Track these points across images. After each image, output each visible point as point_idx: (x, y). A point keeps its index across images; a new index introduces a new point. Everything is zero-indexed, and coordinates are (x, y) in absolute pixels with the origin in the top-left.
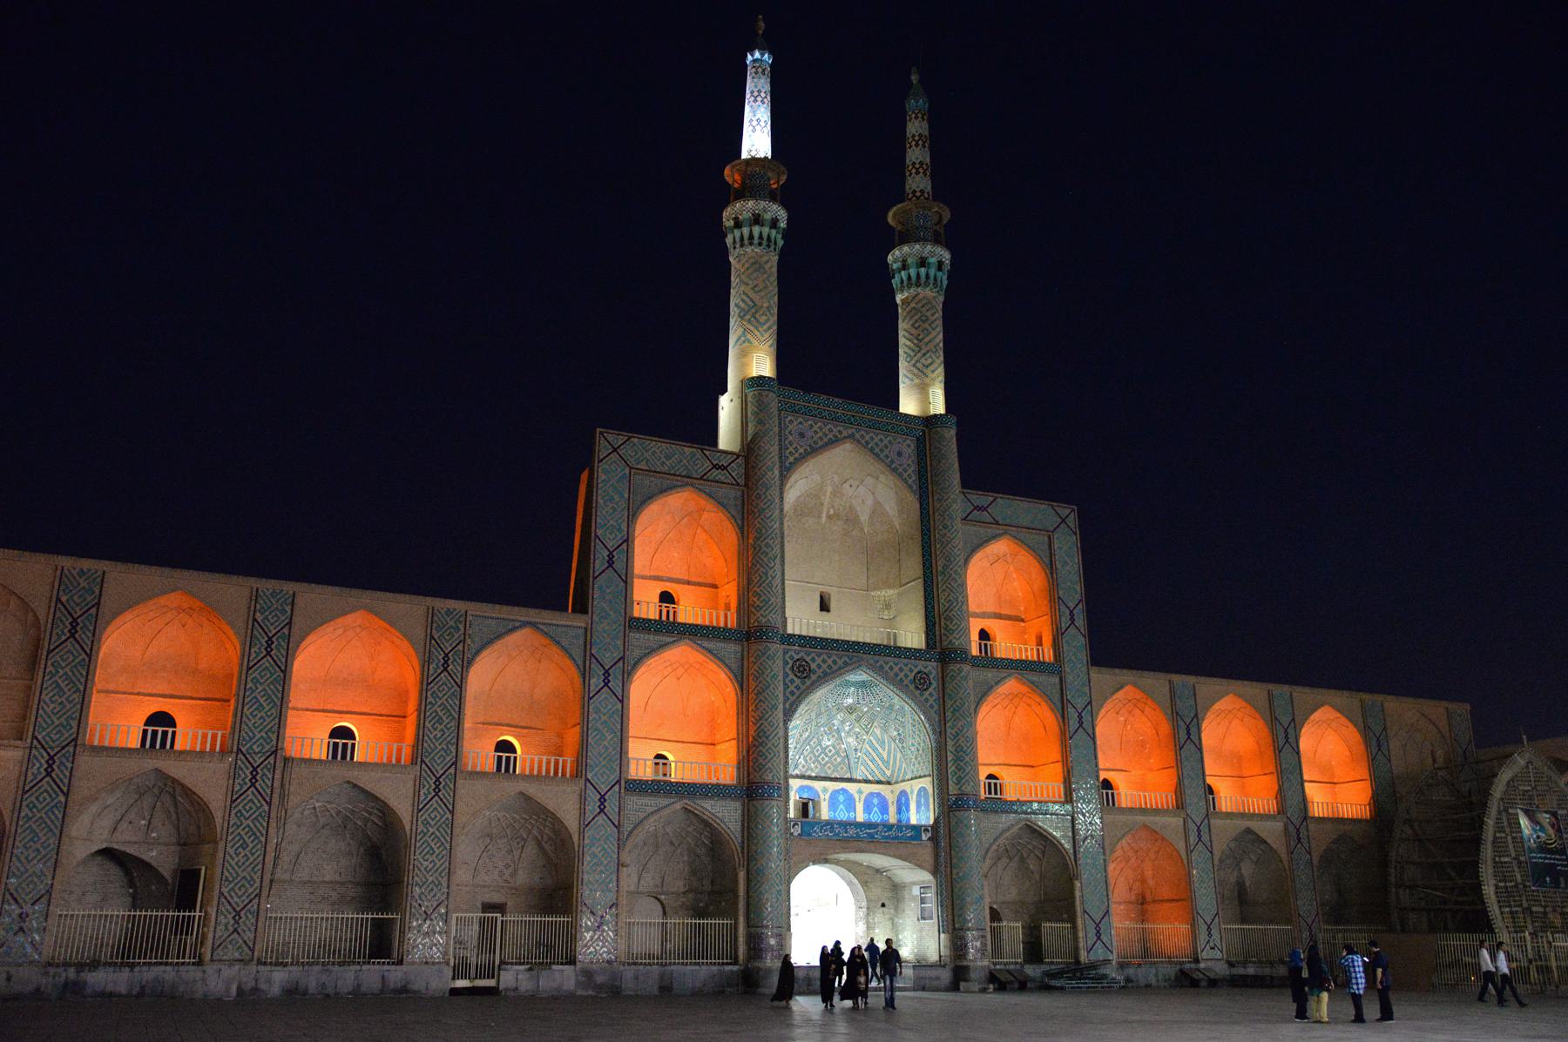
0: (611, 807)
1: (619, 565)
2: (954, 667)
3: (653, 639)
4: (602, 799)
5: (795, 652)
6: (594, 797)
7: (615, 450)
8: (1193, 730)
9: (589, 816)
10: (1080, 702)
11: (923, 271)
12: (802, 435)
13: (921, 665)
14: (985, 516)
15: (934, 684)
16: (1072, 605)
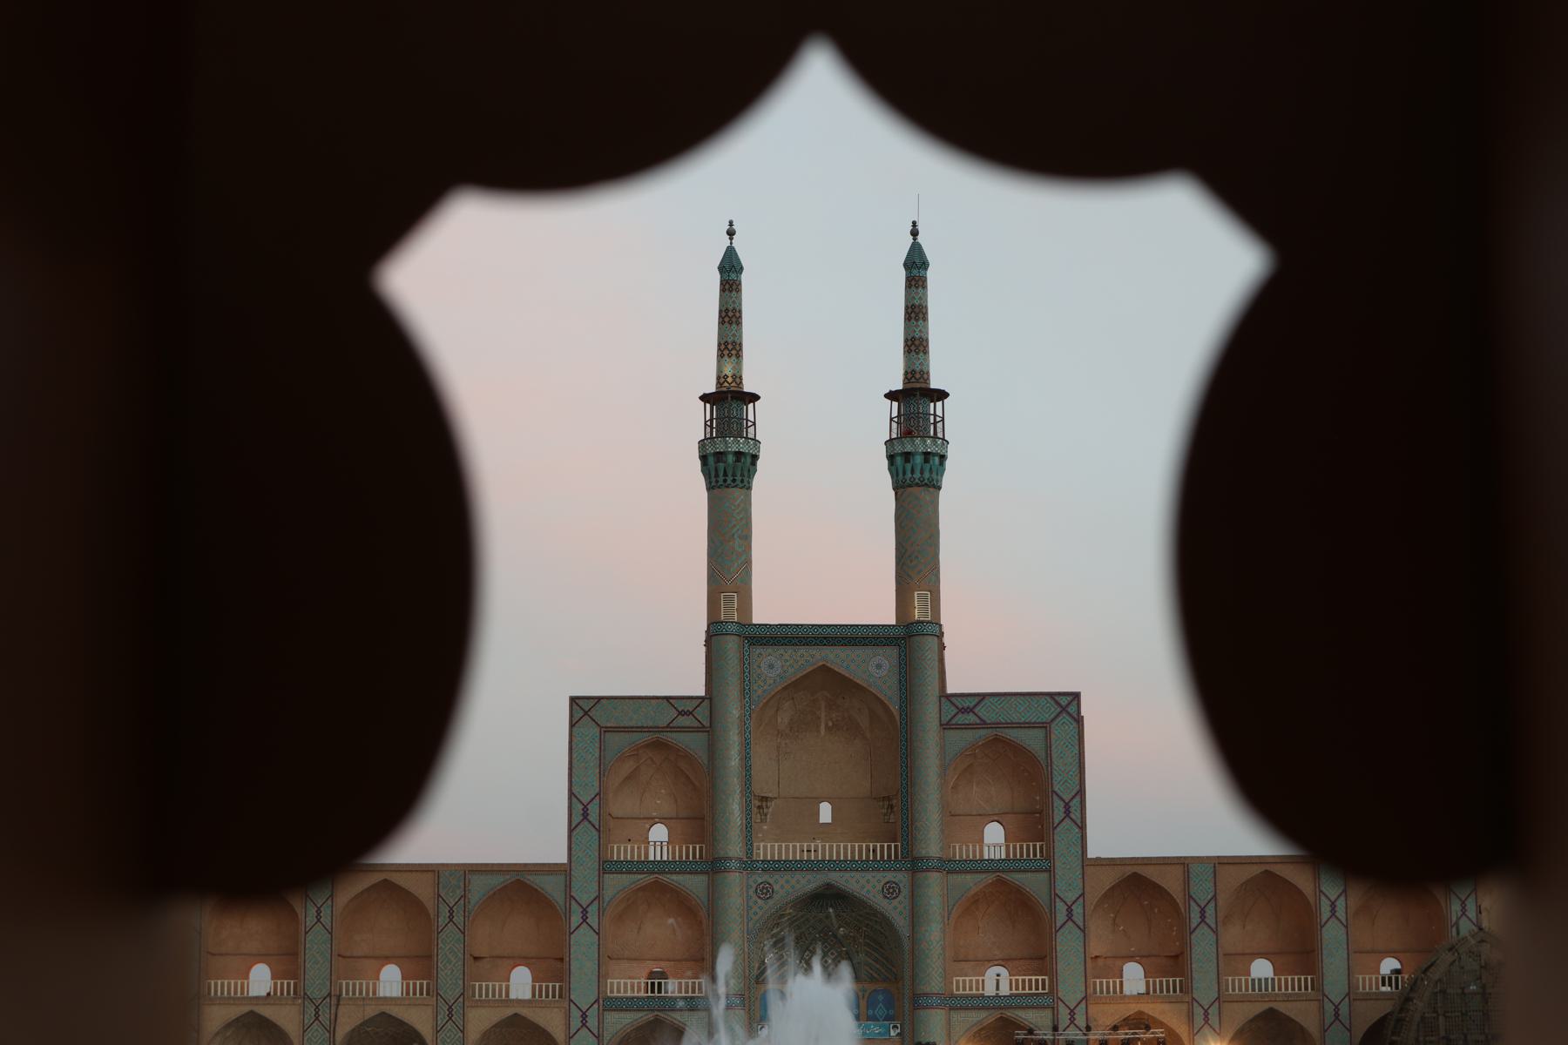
0: (592, 1022)
1: (593, 817)
2: (920, 875)
3: (625, 880)
4: (584, 1016)
5: (760, 878)
6: (576, 1014)
7: (586, 713)
8: (1210, 911)
9: (573, 1031)
10: (1070, 897)
11: (908, 467)
12: (771, 666)
13: (890, 876)
14: (971, 718)
15: (905, 892)
16: (1067, 797)
